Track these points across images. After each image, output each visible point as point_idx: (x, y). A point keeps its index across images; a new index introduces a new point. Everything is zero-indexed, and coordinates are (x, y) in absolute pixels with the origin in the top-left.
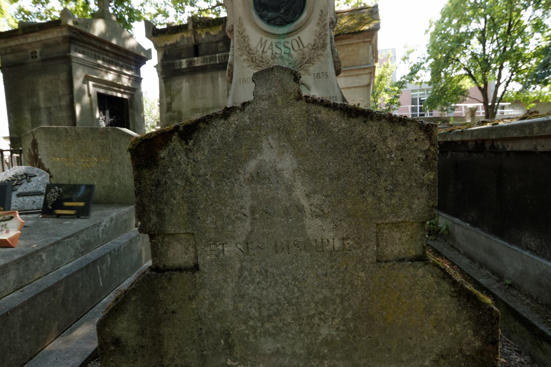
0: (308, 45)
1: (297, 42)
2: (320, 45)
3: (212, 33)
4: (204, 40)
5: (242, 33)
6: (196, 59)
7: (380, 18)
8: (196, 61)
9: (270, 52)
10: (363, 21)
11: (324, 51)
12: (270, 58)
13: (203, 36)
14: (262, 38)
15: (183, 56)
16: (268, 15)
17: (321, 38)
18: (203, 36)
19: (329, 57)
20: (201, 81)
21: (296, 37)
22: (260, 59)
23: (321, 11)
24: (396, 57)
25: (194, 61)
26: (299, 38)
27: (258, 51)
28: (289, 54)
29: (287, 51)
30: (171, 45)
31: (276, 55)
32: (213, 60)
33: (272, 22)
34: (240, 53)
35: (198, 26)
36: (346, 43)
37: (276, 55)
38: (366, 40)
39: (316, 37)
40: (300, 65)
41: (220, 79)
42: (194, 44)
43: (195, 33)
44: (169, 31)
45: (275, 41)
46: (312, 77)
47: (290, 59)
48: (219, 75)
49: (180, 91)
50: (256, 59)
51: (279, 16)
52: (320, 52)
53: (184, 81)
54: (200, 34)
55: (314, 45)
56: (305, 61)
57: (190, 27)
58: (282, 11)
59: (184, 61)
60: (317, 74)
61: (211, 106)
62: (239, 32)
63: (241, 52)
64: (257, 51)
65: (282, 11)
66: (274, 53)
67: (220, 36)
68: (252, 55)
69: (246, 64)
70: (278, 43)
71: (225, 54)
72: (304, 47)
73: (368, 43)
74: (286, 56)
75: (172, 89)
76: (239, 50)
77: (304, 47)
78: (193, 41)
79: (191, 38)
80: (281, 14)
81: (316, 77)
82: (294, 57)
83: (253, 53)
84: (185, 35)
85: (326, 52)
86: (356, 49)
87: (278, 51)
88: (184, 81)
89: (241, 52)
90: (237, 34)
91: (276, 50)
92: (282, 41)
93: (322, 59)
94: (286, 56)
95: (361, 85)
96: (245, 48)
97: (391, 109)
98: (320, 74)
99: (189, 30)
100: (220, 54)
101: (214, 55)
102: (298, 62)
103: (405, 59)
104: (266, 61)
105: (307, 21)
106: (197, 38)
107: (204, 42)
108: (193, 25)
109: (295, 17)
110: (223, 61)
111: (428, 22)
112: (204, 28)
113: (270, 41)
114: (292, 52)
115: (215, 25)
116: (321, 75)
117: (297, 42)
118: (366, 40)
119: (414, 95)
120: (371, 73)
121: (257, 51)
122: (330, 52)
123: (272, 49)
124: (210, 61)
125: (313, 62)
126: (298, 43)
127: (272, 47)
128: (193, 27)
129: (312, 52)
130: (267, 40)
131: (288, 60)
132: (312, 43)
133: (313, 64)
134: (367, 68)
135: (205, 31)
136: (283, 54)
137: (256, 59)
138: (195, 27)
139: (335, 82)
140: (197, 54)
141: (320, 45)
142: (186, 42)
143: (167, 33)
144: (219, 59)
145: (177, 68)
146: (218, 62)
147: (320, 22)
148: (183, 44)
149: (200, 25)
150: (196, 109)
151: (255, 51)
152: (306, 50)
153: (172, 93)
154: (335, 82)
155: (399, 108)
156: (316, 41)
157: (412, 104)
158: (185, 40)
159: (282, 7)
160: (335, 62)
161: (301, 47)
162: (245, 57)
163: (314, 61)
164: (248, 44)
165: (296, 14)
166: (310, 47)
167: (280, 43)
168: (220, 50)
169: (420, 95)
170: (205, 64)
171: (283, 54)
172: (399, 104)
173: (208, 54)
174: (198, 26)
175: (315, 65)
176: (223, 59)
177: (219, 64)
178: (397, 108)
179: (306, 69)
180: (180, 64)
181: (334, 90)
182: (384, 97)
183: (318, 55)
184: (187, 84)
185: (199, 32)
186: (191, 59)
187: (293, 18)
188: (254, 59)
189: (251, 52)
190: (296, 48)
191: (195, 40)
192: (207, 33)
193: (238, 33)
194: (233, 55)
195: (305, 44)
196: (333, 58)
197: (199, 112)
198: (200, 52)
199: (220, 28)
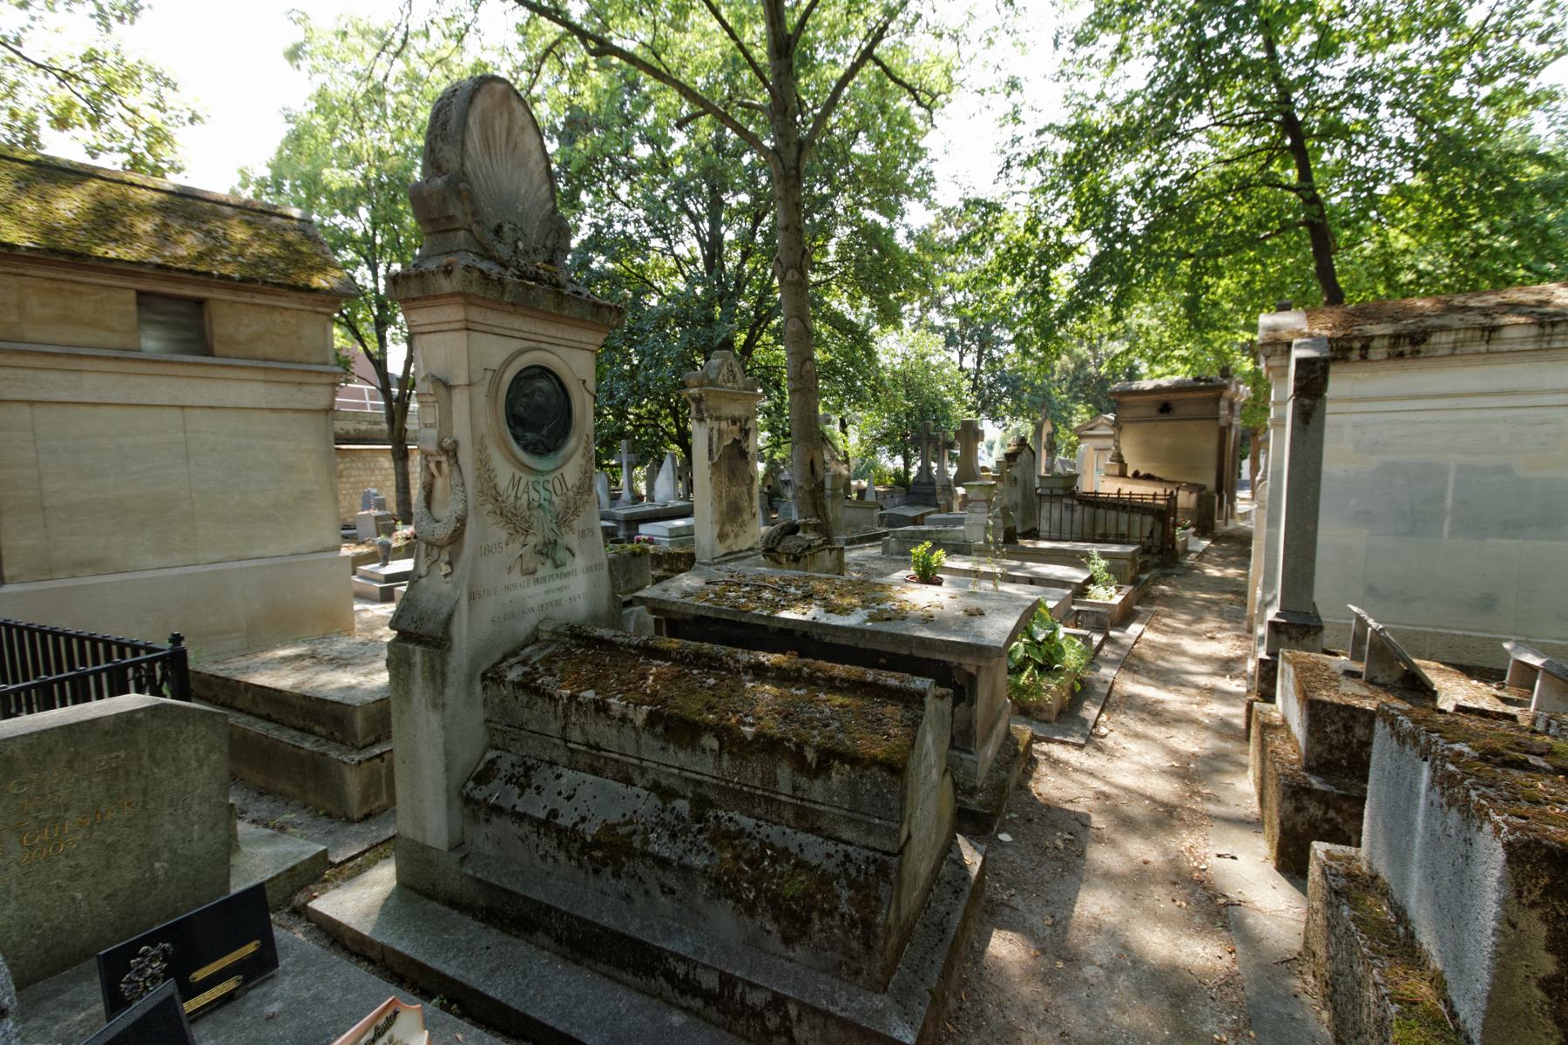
9: (525, 497)
21: (558, 474)
28: (550, 502)
36: (266, 302)
38: (320, 309)
45: (532, 478)
46: (576, 536)
58: (544, 432)
65: (544, 432)
69: (490, 520)
73: (325, 317)
74: (546, 504)
86: (293, 321)
91: (534, 495)
92: (541, 479)
95: (309, 407)
113: (527, 478)
114: (554, 498)
118: (320, 309)
134: (327, 373)
162: (489, 507)
195: (569, 486)
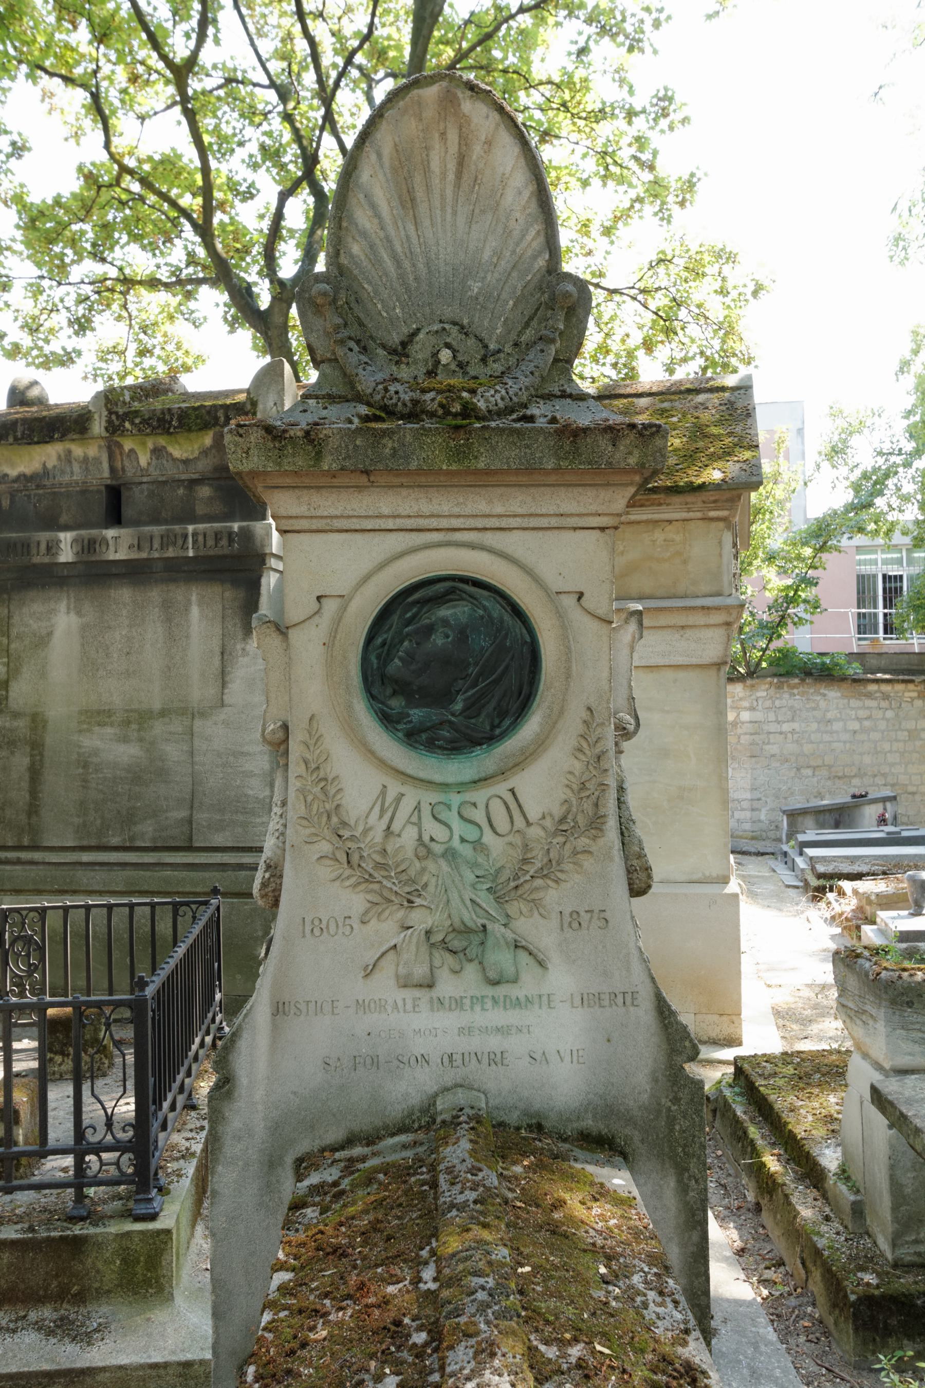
0: (544, 817)
1: (505, 803)
2: (581, 820)
3: (177, 452)
4: (144, 472)
5: (318, 768)
6: (110, 533)
7: (762, 437)
8: (111, 542)
9: (410, 834)
10: (701, 444)
11: (595, 838)
12: (410, 853)
13: (144, 460)
14: (385, 787)
15: (64, 519)
16: (408, 715)
17: (588, 797)
18: (144, 460)
19: (611, 859)
20: (124, 612)
21: (501, 789)
22: (378, 858)
23: (589, 709)
24: (806, 431)
25: (104, 541)
26: (512, 791)
27: (370, 829)
28: (478, 845)
29: (471, 833)
30: (22, 477)
31: (433, 845)
32: (174, 544)
33: (424, 736)
34: (308, 831)
35: (127, 425)
36: (644, 517)
37: (433, 845)
38: (712, 514)
39: (569, 792)
40: (513, 884)
41: (195, 611)
42: (109, 482)
43: (112, 448)
44: (19, 434)
45: (430, 797)
46: (555, 922)
47: (480, 860)
48: (194, 598)
49: (42, 641)
50: (361, 857)
51: (450, 722)
52: (583, 841)
53: (63, 606)
54: (132, 451)
55: (563, 820)
56: (531, 873)
57: (98, 427)
58: (458, 706)
59: (66, 537)
60: (571, 914)
61: (157, 706)
62: (306, 762)
63: (313, 830)
64: (366, 831)
65: (458, 706)
66: (426, 838)
67: (205, 465)
68: (349, 844)
69: (326, 872)
70: (441, 807)
71: (217, 525)
72: (529, 824)
73: (721, 525)
74: (466, 851)
75: (14, 632)
76: (304, 822)
77: (529, 824)
78: (106, 474)
79: (97, 460)
80: (453, 715)
81: (566, 925)
82: (494, 854)
83: (352, 838)
84: (78, 451)
85: (601, 842)
86: (678, 538)
87: (440, 833)
88: (63, 606)
89: (313, 830)
90: (302, 769)
91: (431, 828)
92: (455, 799)
93: (587, 863)
94: (466, 851)
95: (694, 661)
96: (325, 819)
97: (789, 621)
98: (582, 913)
99: (92, 438)
100: (201, 526)
101: (177, 528)
102: (506, 874)
103: (836, 452)
104: (397, 866)
105: (540, 745)
106: (119, 465)
107: (145, 479)
108: (110, 422)
109: (498, 726)
110: (211, 553)
111: (909, 337)
112: (147, 435)
113: (412, 797)
114: (488, 837)
115: (190, 430)
116: (585, 917)
117: (505, 803)
118: (712, 514)
119: (865, 562)
120: (728, 624)
121: (366, 831)
122: (617, 844)
123: (419, 825)
124: (163, 547)
125: (559, 875)
126: (508, 808)
127: (420, 818)
128: (106, 429)
129: (555, 841)
130: (403, 795)
131: (474, 865)
132: (558, 812)
133: (557, 881)
134: (717, 608)
135: (150, 445)
136: (456, 842)
137: (361, 857)
138: (114, 428)
139: (632, 945)
140: (115, 517)
141: (581, 820)
142: (77, 473)
143: (11, 440)
144: (195, 542)
145: (36, 560)
146: (191, 553)
147: (585, 745)
148: (66, 478)
149: (132, 423)
150: (99, 712)
151: (361, 829)
152: (535, 832)
153: (13, 646)
154: (632, 945)
155: (815, 618)
156: (571, 806)
157: (859, 608)
158: (76, 468)
159: (458, 692)
160: (630, 871)
161: (519, 823)
162: (325, 847)
163: (562, 871)
164: (338, 806)
165: (502, 714)
166: (548, 823)
167: (449, 807)
168: (200, 510)
169: (885, 562)
170: (144, 555)
171: (456, 842)
172: (815, 605)
173: (156, 520)
174: (127, 425)
175: (563, 885)
176: (211, 542)
177: (194, 558)
178: (807, 616)
179: (534, 896)
180: (52, 548)
181: (628, 970)
182: (763, 577)
183: (575, 853)
184: (74, 619)
185: (128, 444)
186: (94, 532)
187: (493, 728)
188: (355, 858)
189: (346, 833)
190: (502, 823)
191: (112, 469)
192: (158, 452)
193: (303, 767)
194: (283, 834)
195: (533, 814)
196: (626, 858)
197: (112, 725)
198: (128, 512)
199: (208, 440)
